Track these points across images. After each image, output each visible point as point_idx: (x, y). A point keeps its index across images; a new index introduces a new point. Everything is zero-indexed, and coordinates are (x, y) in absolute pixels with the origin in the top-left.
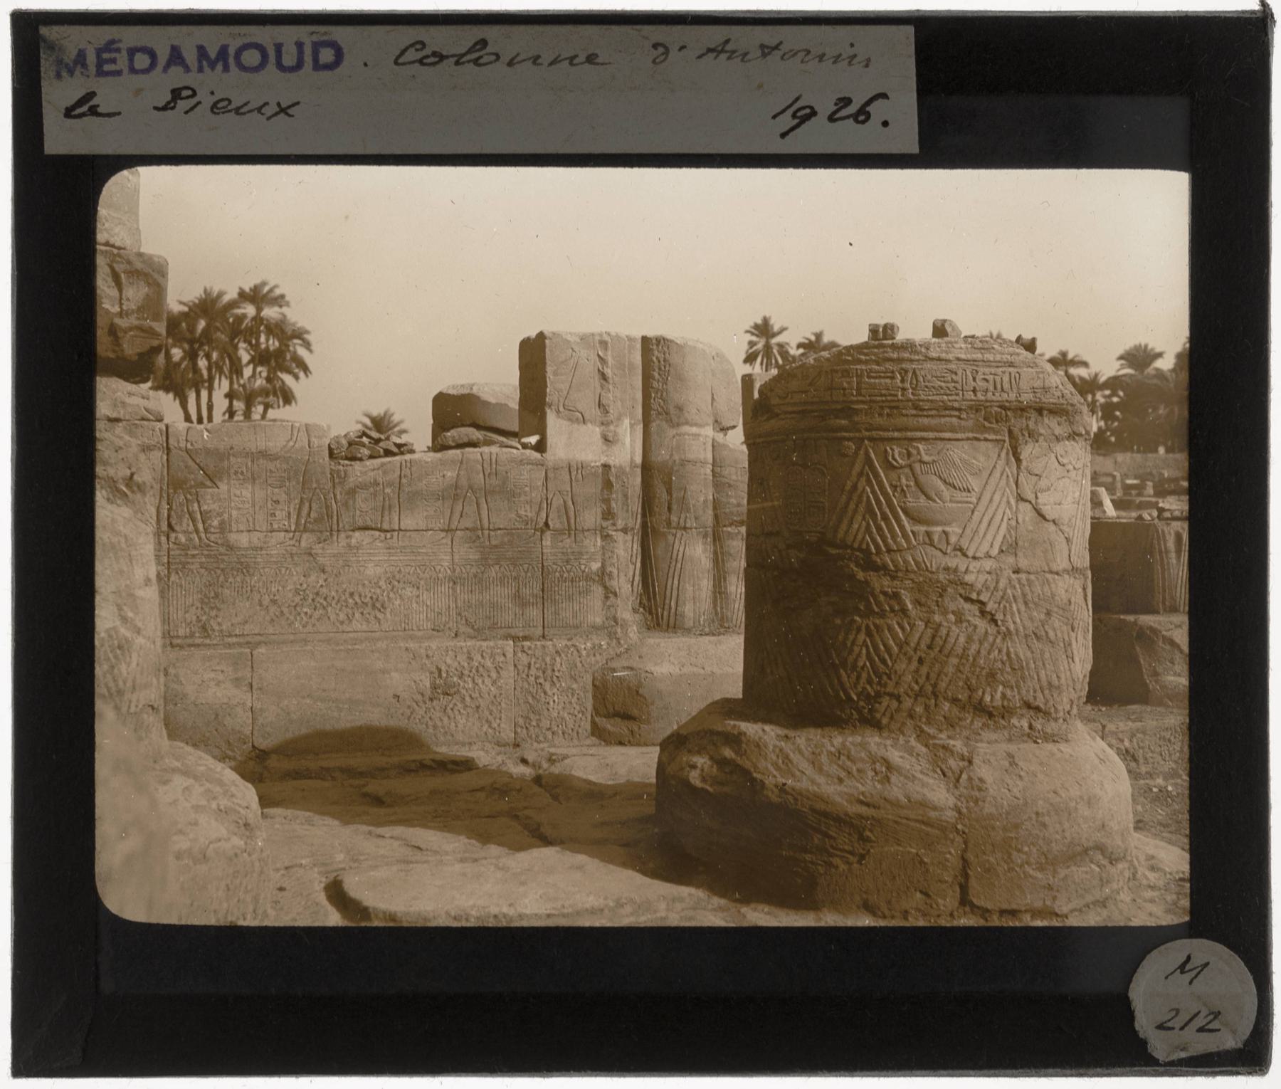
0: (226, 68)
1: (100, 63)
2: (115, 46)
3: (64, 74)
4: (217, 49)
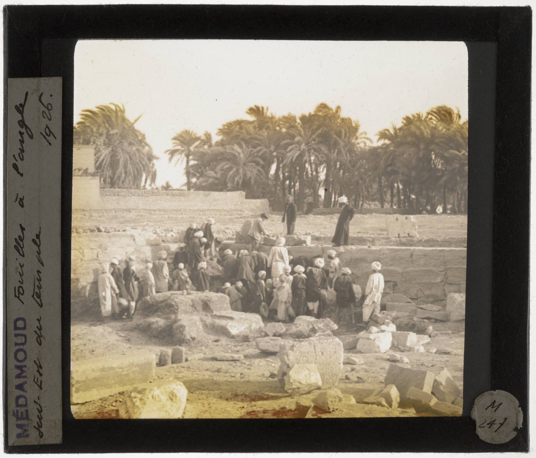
0: (25, 366)
1: (22, 418)
2: (15, 411)
4: (16, 370)
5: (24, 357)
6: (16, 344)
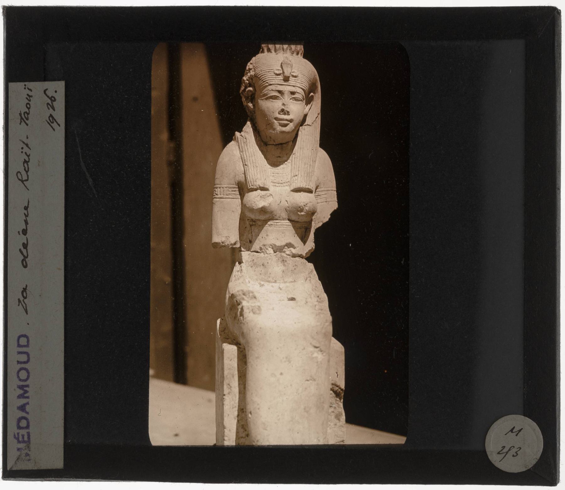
0: (27, 386)
1: (24, 442)
5: (26, 374)
6: (19, 362)
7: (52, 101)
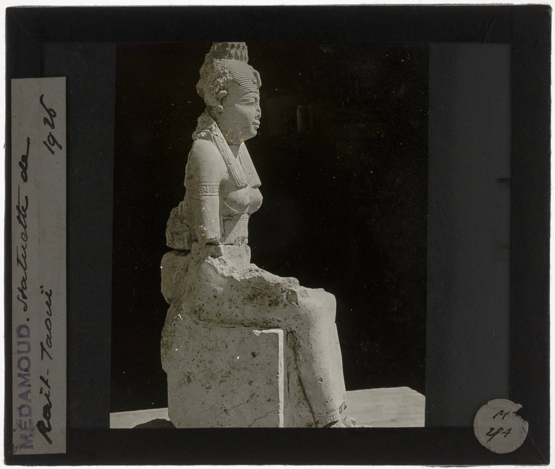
3: (30, 444)
7: (52, 116)
